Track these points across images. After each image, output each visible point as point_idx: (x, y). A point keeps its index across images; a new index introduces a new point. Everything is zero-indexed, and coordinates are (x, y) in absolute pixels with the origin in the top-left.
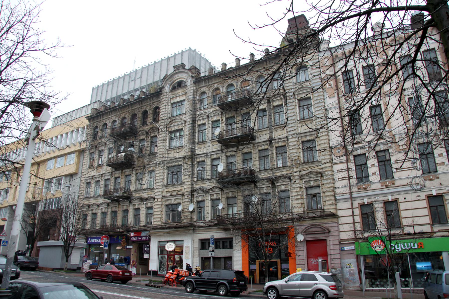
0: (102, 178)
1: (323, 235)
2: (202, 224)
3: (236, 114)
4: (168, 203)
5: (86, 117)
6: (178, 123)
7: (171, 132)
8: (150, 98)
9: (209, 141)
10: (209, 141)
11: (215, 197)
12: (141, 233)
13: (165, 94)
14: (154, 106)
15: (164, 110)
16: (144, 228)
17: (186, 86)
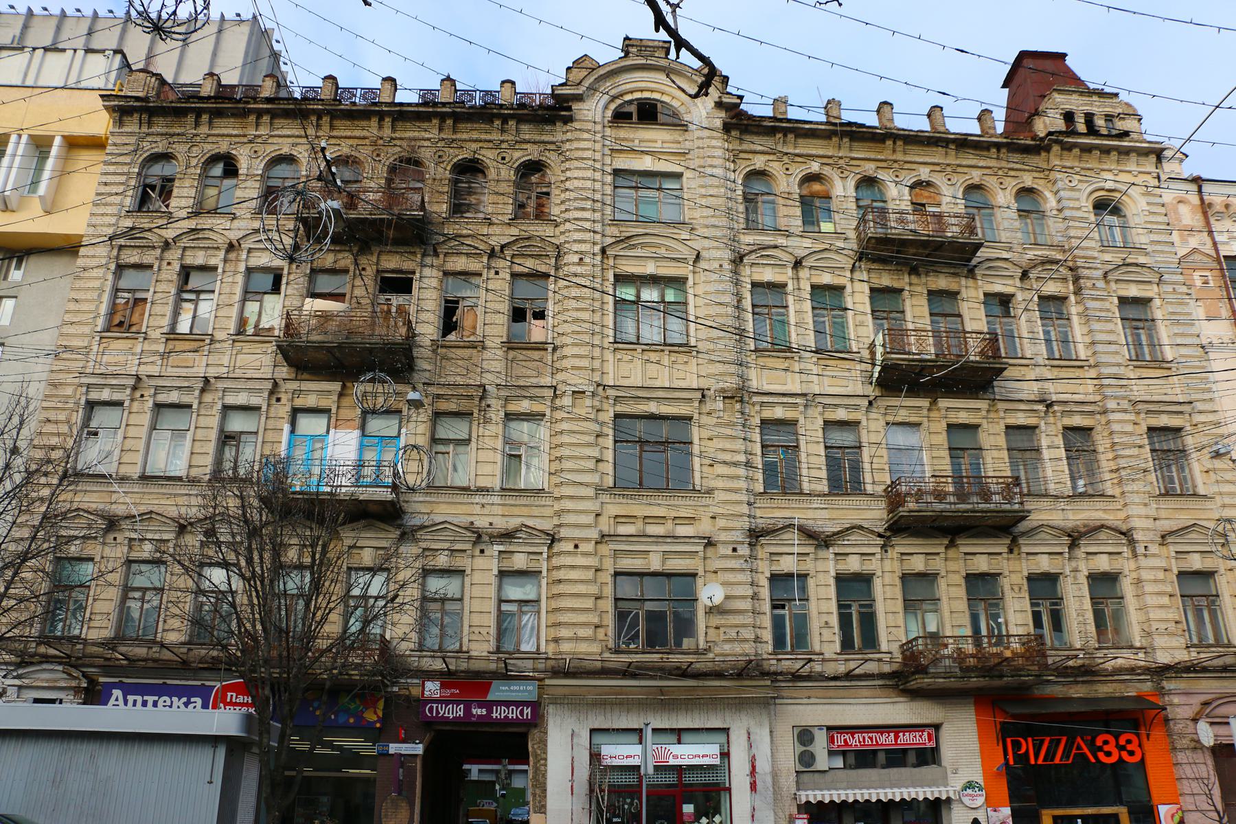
0: (208, 398)
4: (627, 564)
5: (101, 96)
7: (620, 279)
11: (853, 565)
12: (486, 688)
13: (590, 126)
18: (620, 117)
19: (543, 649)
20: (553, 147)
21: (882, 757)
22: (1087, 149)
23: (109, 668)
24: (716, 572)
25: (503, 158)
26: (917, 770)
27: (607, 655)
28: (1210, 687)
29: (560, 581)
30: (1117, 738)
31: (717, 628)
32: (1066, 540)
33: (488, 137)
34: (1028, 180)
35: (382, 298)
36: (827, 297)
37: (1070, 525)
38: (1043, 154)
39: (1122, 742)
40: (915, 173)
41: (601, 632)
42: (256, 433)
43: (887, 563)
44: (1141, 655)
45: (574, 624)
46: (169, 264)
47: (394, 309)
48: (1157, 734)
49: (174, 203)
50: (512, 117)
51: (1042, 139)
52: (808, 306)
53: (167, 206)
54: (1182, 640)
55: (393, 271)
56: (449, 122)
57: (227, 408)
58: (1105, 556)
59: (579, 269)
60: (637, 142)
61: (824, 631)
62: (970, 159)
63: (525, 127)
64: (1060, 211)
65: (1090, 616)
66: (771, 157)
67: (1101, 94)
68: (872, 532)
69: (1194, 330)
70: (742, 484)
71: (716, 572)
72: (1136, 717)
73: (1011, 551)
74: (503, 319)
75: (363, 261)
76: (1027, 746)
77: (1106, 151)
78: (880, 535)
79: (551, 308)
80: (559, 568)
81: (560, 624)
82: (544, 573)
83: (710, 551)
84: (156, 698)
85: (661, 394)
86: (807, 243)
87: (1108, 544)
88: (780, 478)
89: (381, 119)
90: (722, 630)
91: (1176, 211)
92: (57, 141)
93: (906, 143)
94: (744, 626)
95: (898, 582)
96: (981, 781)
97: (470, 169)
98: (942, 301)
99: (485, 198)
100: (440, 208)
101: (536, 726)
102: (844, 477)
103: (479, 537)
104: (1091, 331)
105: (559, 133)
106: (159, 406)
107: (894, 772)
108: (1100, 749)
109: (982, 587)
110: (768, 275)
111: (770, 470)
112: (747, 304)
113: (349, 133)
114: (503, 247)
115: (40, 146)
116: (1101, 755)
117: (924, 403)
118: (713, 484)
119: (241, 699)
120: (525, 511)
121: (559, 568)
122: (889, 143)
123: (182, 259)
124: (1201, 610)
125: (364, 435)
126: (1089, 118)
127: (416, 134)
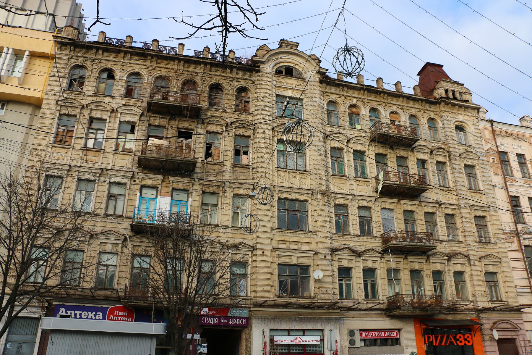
1: (513, 333)
5: (53, 36)
10: (352, 178)
11: (369, 264)
14: (237, 84)
18: (278, 72)
19: (249, 295)
20: (251, 82)
21: (379, 342)
22: (454, 105)
23: (58, 298)
24: (318, 265)
25: (231, 85)
26: (392, 347)
27: (276, 298)
28: (496, 316)
29: (256, 267)
30: (464, 335)
31: (319, 288)
32: (446, 258)
33: (224, 75)
34: (432, 115)
35: (180, 140)
36: (359, 155)
37: (447, 252)
38: (438, 105)
39: (466, 337)
40: (391, 108)
41: (273, 288)
42: (124, 195)
43: (382, 264)
44: (472, 304)
45: (262, 285)
46: (84, 116)
47: (184, 145)
48: (478, 334)
49: (85, 88)
50: (235, 67)
51: (438, 99)
52: (352, 158)
53: (82, 89)
54: (486, 298)
55: (185, 129)
57: (111, 183)
58: (460, 265)
59: (263, 136)
60: (285, 84)
61: (359, 291)
62: (412, 104)
63: (240, 72)
64: (444, 128)
65: (454, 288)
66: (338, 96)
67: (457, 83)
68: (377, 252)
69: (490, 179)
70: (328, 230)
71: (318, 265)
72: (471, 328)
73: (426, 261)
74: (232, 153)
75: (173, 123)
76: (432, 338)
77: (460, 106)
78: (380, 253)
79: (251, 151)
80: (256, 261)
81: (256, 285)
82: (250, 263)
83: (316, 256)
84: (81, 312)
85: (297, 191)
86: (351, 132)
87: (460, 260)
88: (341, 228)
89: (179, 62)
90: (321, 289)
91: (484, 133)
92: (27, 53)
93: (388, 96)
94: (329, 288)
95: (386, 272)
96: (416, 352)
97: (216, 88)
98: (402, 160)
99: (223, 101)
100: (204, 104)
101: (247, 327)
102: (365, 228)
103: (224, 246)
104: (455, 177)
105: (254, 76)
106: (79, 180)
107: (384, 348)
108: (458, 340)
109: (416, 274)
110: (337, 145)
111: (338, 224)
112: (329, 156)
113: (163, 66)
114: (232, 123)
115: (18, 54)
116: (458, 342)
117: (395, 201)
118: (317, 229)
119: (121, 314)
120: (241, 236)
121: (256, 261)
122: (382, 95)
123: (90, 114)
124: (491, 287)
125: (172, 199)
126: (454, 92)
127: (194, 70)
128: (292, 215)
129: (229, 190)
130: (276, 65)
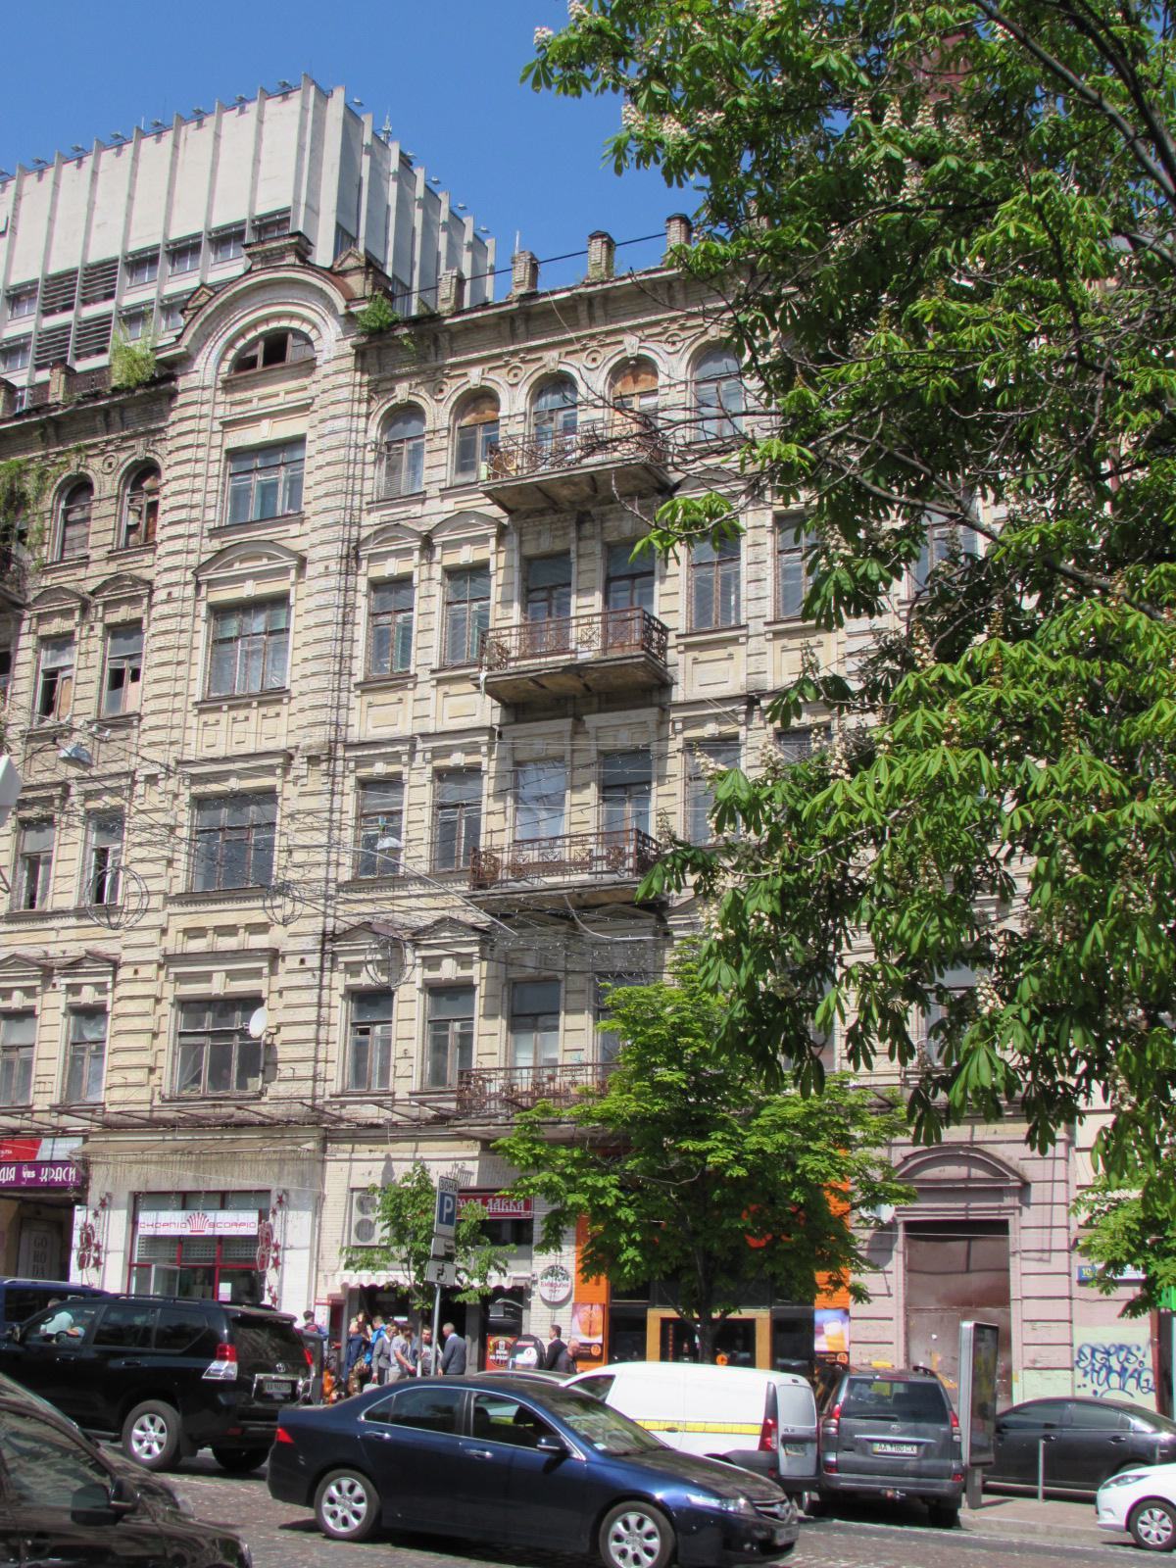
2: (369, 1113)
3: (580, 539)
6: (263, 564)
7: (220, 612)
8: (106, 412)
9: (424, 675)
10: (424, 675)
12: (36, 1144)
13: (194, 396)
15: (186, 484)
16: (54, 1120)
17: (309, 366)
56: (51, 431)
128: (233, 842)
129: (75, 799)
130: (230, 344)
